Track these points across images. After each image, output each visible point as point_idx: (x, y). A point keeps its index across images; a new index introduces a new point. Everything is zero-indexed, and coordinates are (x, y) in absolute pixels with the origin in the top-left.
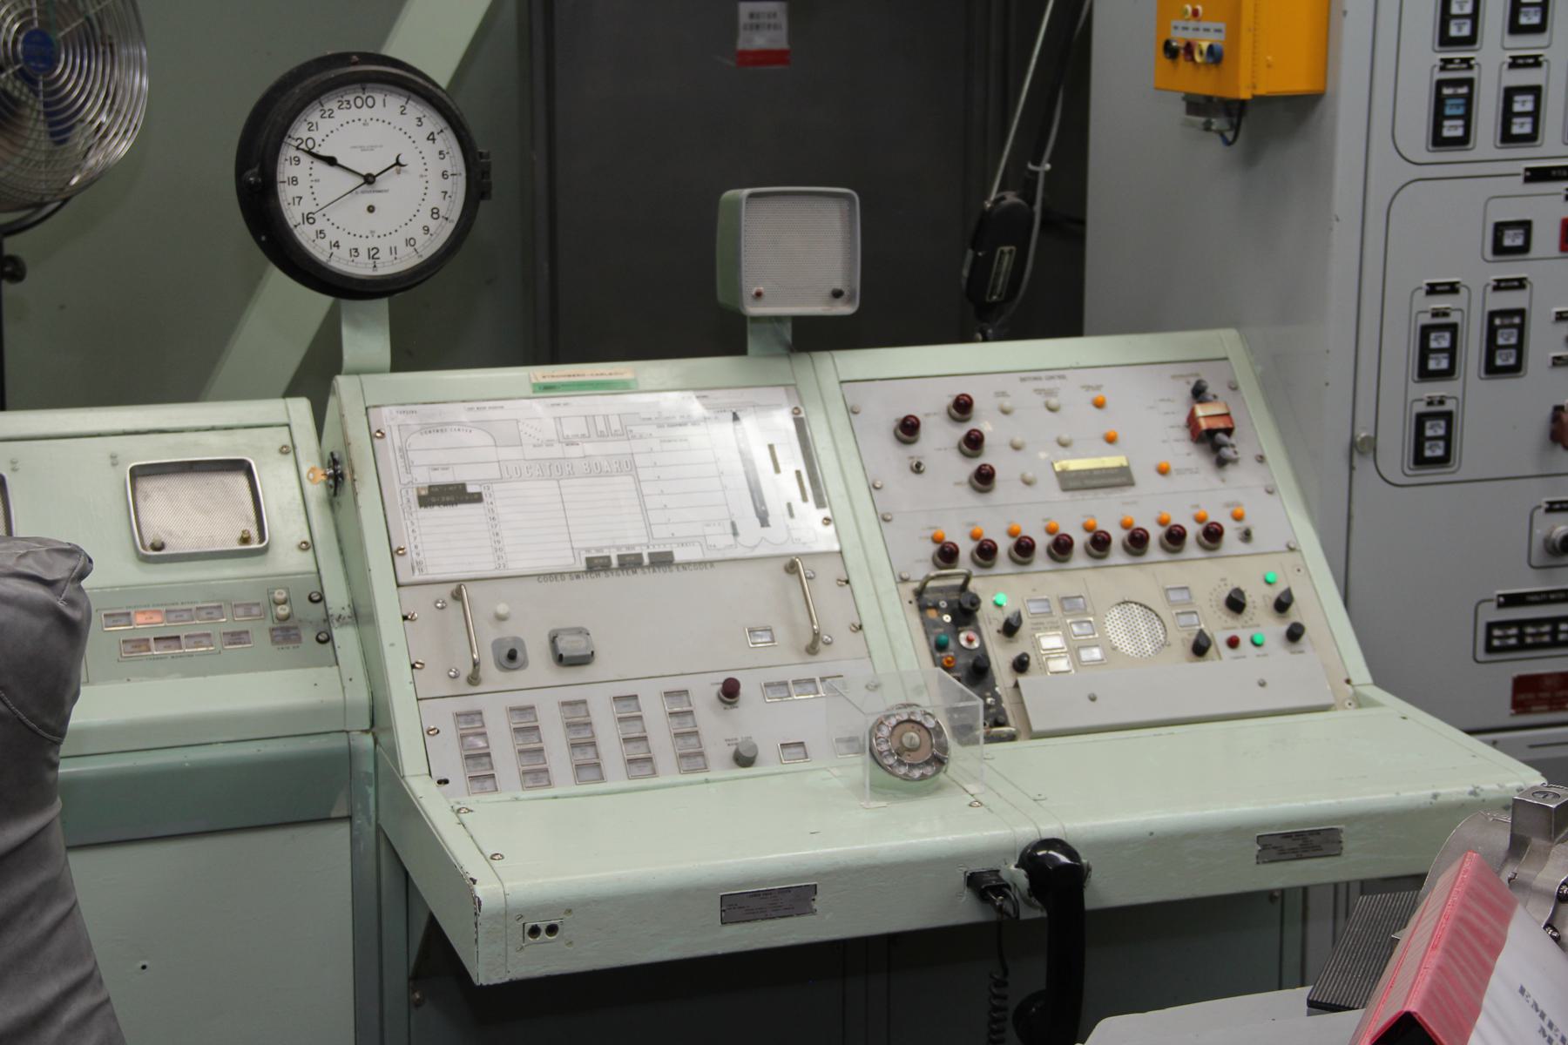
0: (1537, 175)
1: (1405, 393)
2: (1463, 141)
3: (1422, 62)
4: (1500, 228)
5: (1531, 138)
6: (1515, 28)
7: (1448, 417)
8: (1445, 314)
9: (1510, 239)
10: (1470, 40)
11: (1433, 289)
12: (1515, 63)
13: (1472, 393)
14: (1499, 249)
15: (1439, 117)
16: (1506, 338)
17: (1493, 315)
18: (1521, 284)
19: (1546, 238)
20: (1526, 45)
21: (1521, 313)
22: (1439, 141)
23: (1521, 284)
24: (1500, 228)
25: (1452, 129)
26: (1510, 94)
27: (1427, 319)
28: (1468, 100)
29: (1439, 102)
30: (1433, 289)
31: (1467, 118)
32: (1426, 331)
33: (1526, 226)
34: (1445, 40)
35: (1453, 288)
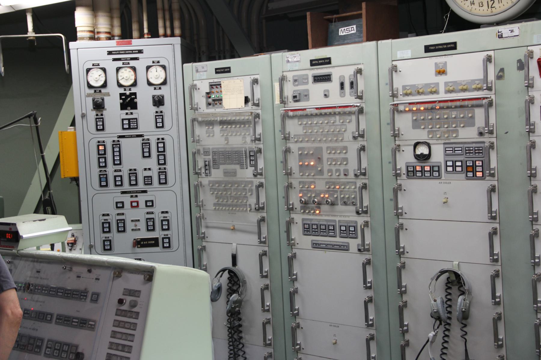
0: (123, 193)
1: (99, 237)
2: (107, 186)
3: (96, 171)
4: (117, 203)
5: (121, 185)
6: (115, 164)
7: (110, 241)
8: (107, 220)
9: (120, 205)
10: (105, 166)
11: (104, 215)
12: (115, 171)
13: (114, 235)
14: (117, 207)
15: (100, 182)
16: (121, 225)
17: (117, 220)
18: (123, 214)
19: (127, 205)
20: (118, 167)
21: (124, 220)
22: (101, 186)
23: (123, 214)
24: (117, 203)
25: (104, 184)
26: (115, 177)
27: (103, 221)
28: (106, 178)
29: (100, 178)
30: (104, 215)
31: (107, 181)
32: (103, 223)
33: (123, 203)
34: (100, 167)
35: (108, 215)
